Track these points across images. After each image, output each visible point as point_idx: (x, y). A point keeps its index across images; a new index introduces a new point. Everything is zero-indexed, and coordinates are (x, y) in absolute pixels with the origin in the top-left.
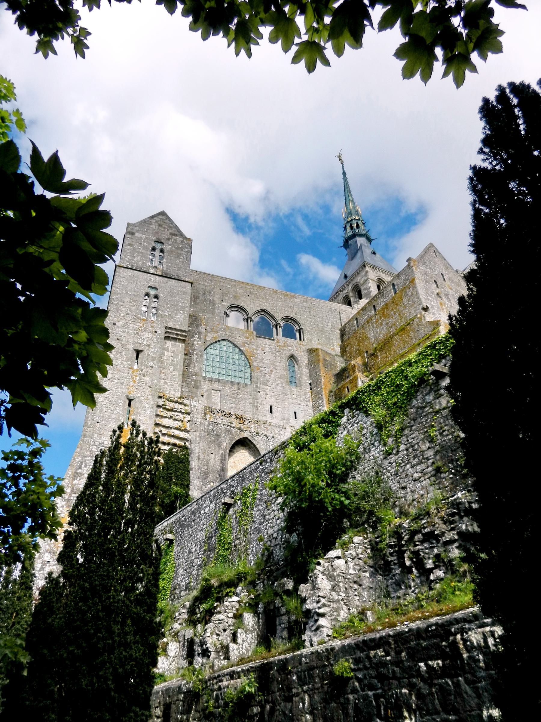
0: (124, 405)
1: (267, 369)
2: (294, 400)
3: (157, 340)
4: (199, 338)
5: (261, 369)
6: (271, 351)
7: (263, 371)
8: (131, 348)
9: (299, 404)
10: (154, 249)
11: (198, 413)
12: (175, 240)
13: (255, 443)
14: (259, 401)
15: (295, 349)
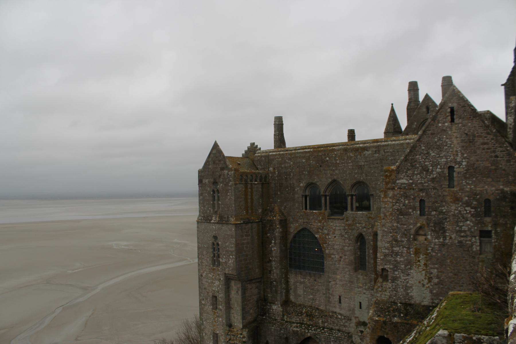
0: (213, 338)
1: (337, 256)
2: (360, 289)
3: (222, 286)
4: (275, 243)
5: (333, 256)
6: (341, 234)
7: (333, 258)
8: (211, 294)
9: (365, 293)
10: (214, 191)
11: (278, 315)
12: (224, 175)
13: (318, 340)
14: (330, 292)
15: (363, 225)
